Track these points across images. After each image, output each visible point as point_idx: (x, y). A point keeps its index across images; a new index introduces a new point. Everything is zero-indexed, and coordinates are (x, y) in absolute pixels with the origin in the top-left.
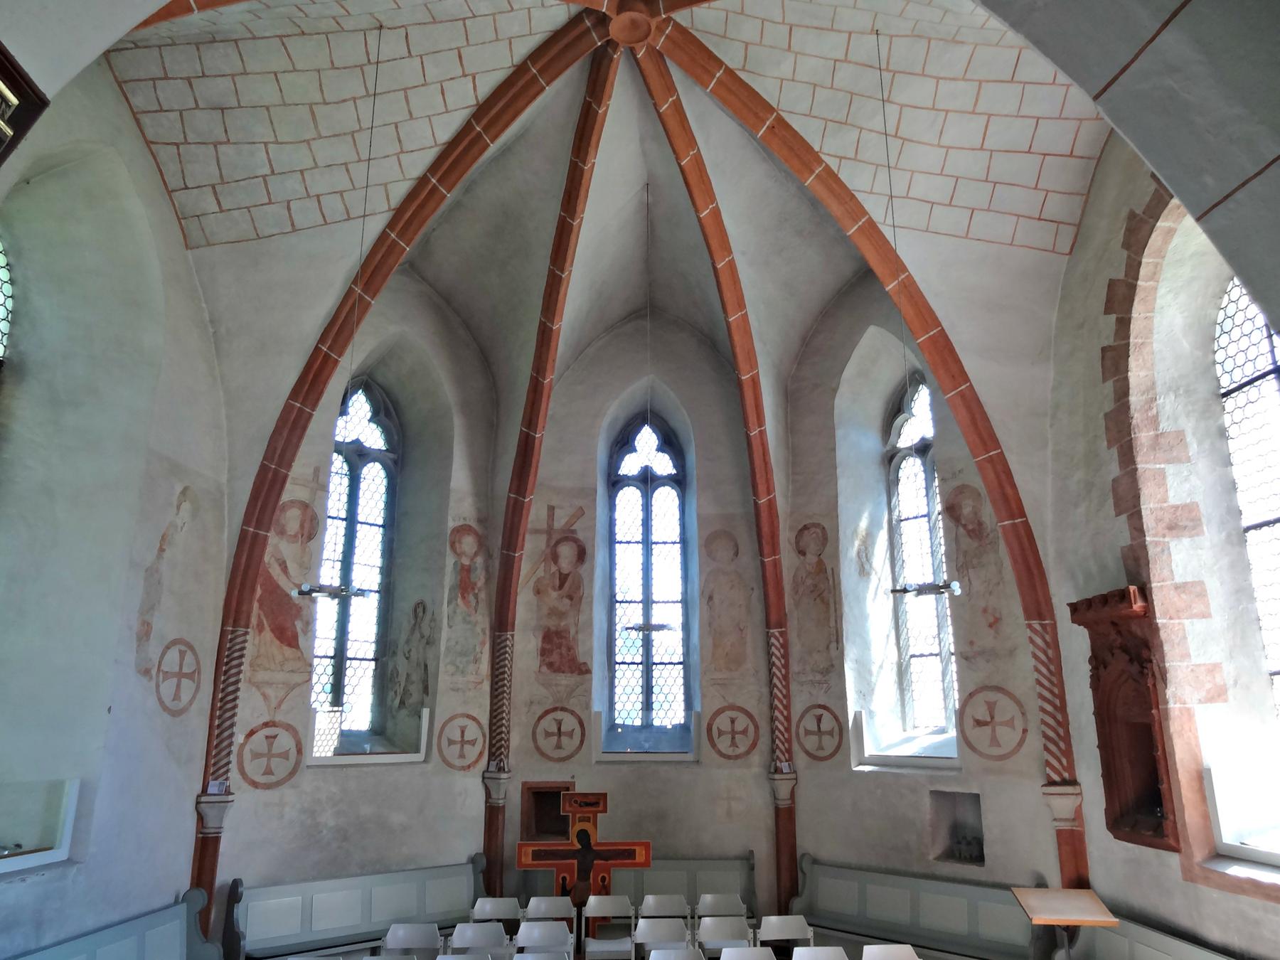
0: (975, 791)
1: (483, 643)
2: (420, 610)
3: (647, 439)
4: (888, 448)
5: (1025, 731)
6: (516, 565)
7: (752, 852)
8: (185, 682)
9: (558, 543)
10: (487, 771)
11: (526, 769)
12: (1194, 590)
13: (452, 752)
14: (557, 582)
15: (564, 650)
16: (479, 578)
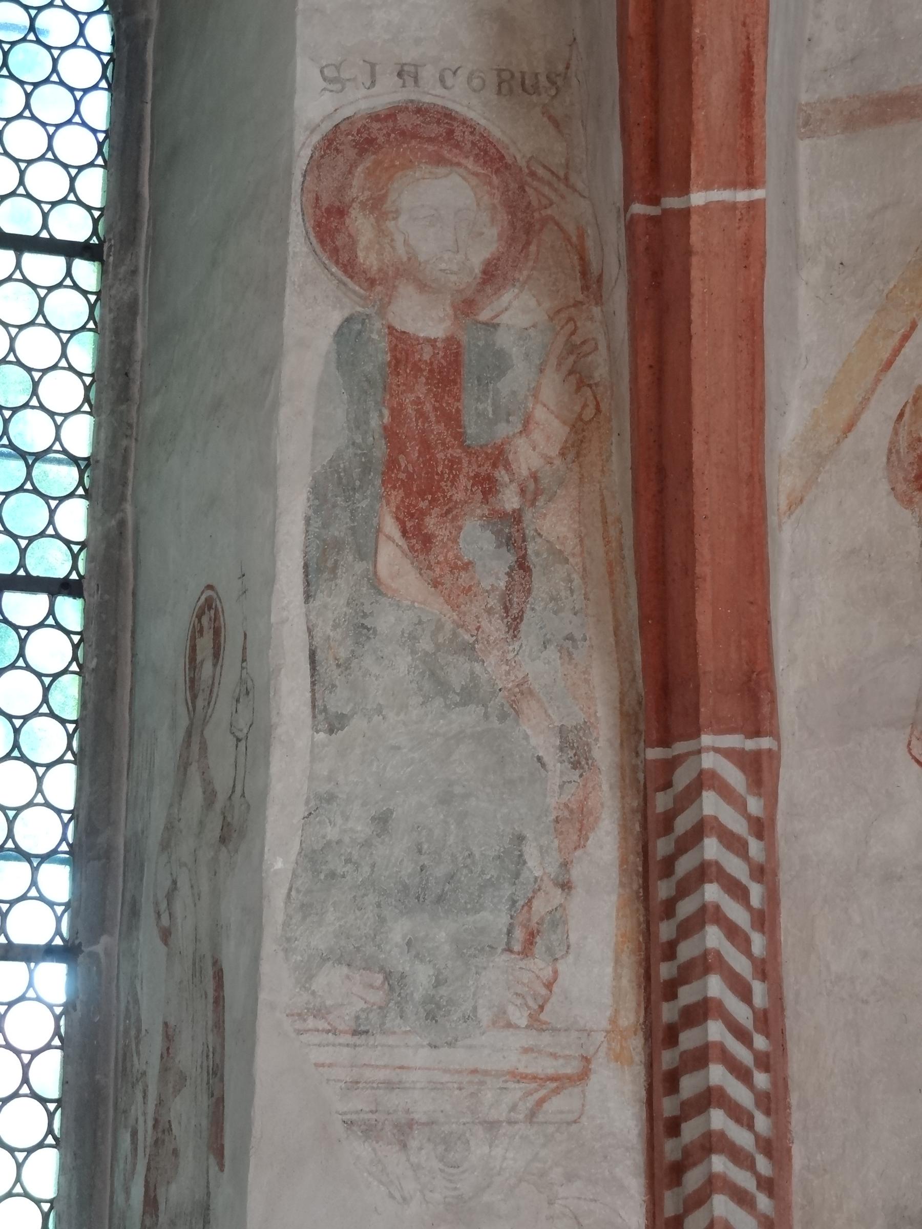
1: (576, 822)
16: (527, 413)
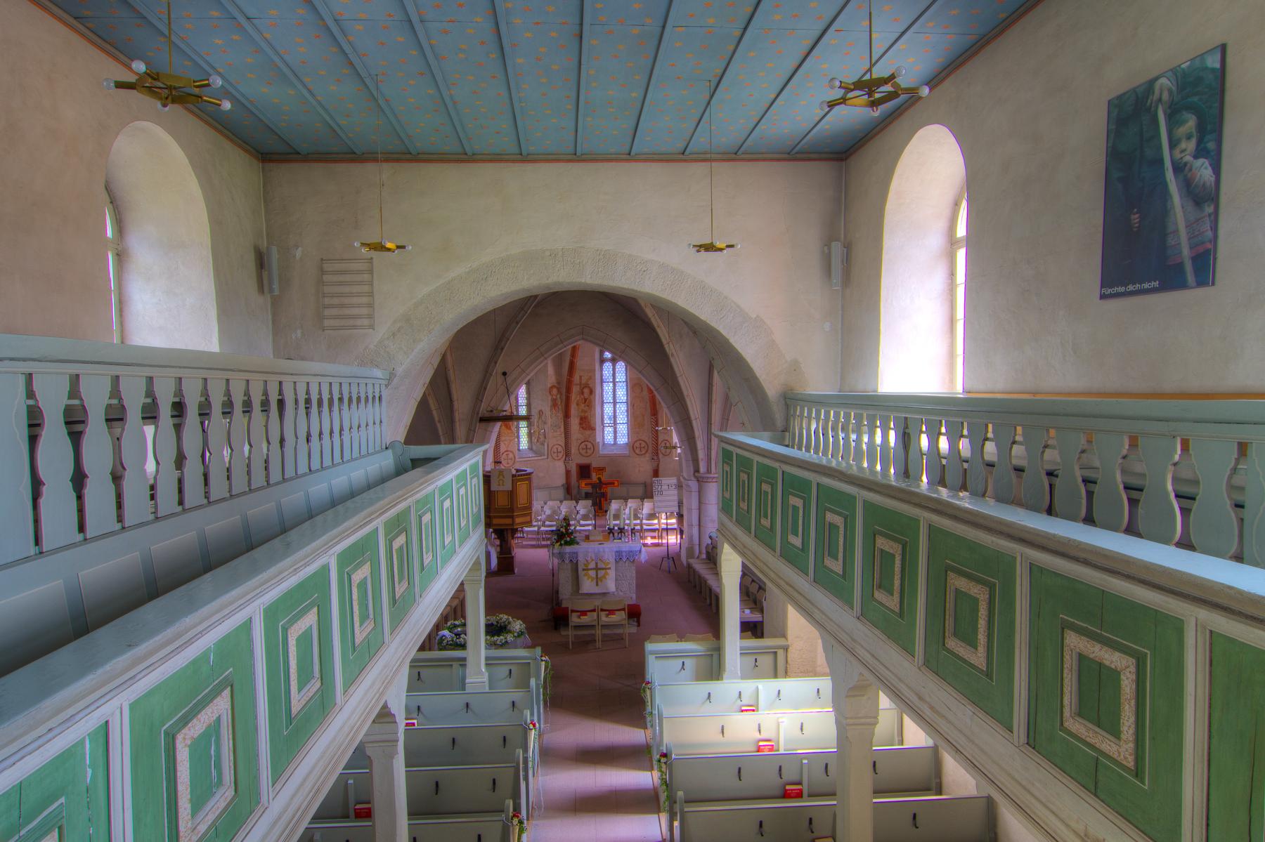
11: (577, 459)
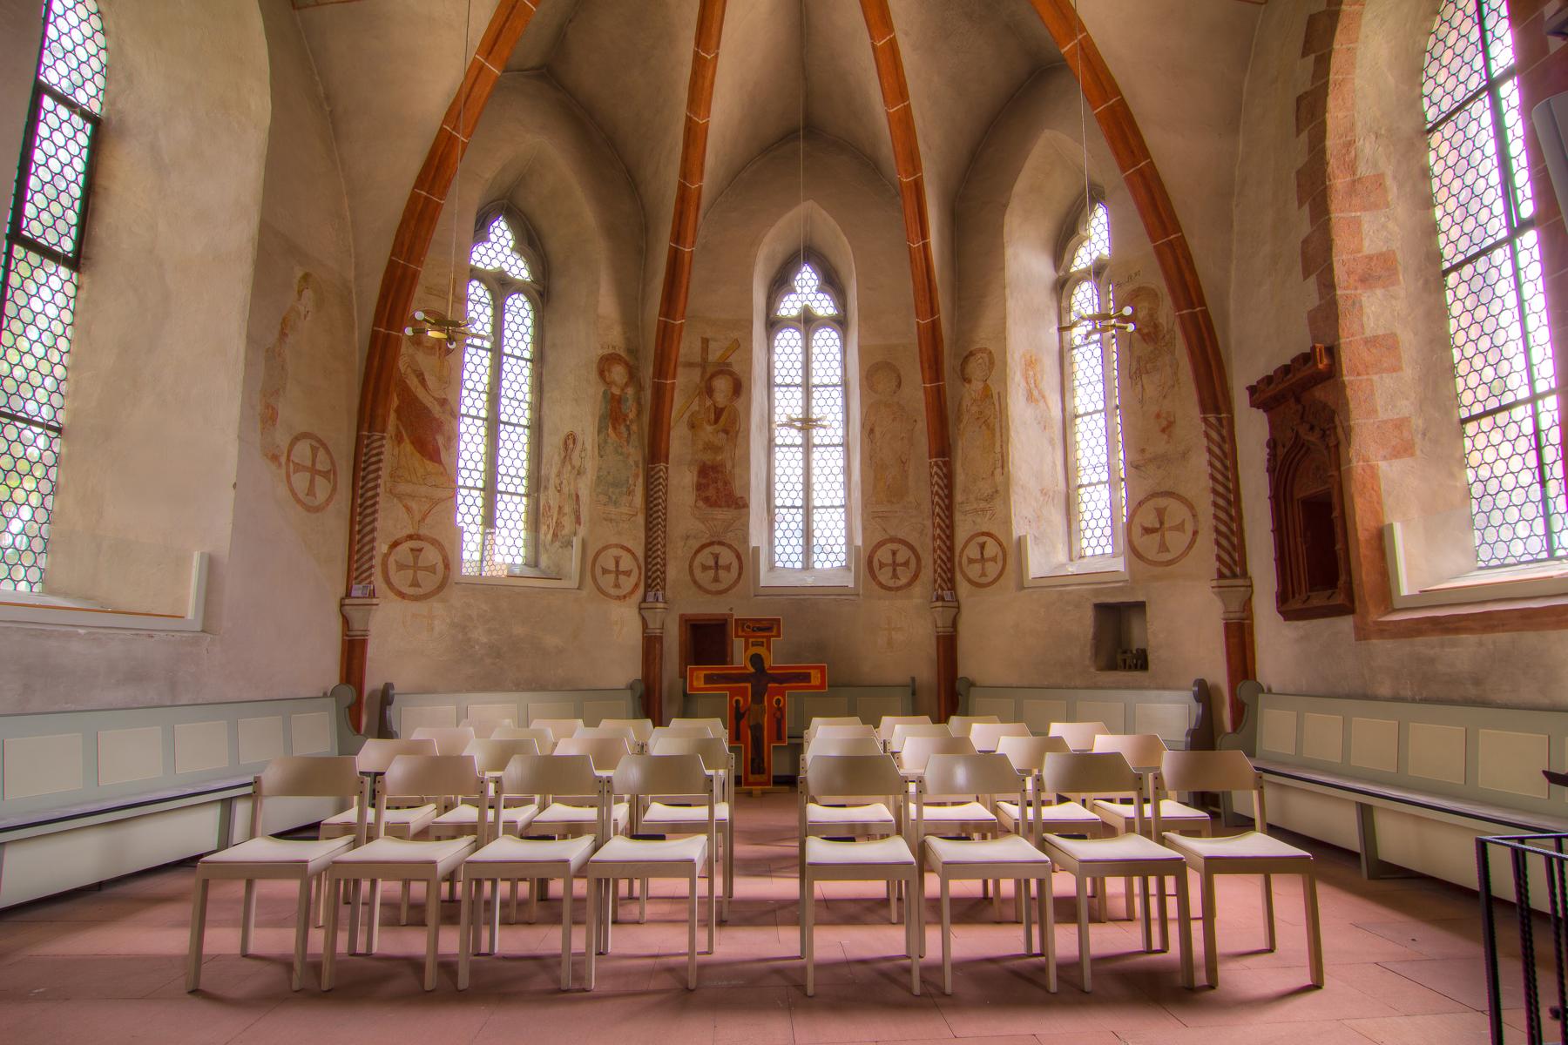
0: (1141, 599)
1: (637, 476)
2: (570, 442)
3: (807, 278)
4: (1061, 273)
5: (1195, 533)
6: (668, 395)
7: (913, 679)
8: (319, 480)
9: (713, 376)
10: (644, 600)
12: (1387, 343)
13: (607, 581)
14: (713, 416)
15: (720, 484)
